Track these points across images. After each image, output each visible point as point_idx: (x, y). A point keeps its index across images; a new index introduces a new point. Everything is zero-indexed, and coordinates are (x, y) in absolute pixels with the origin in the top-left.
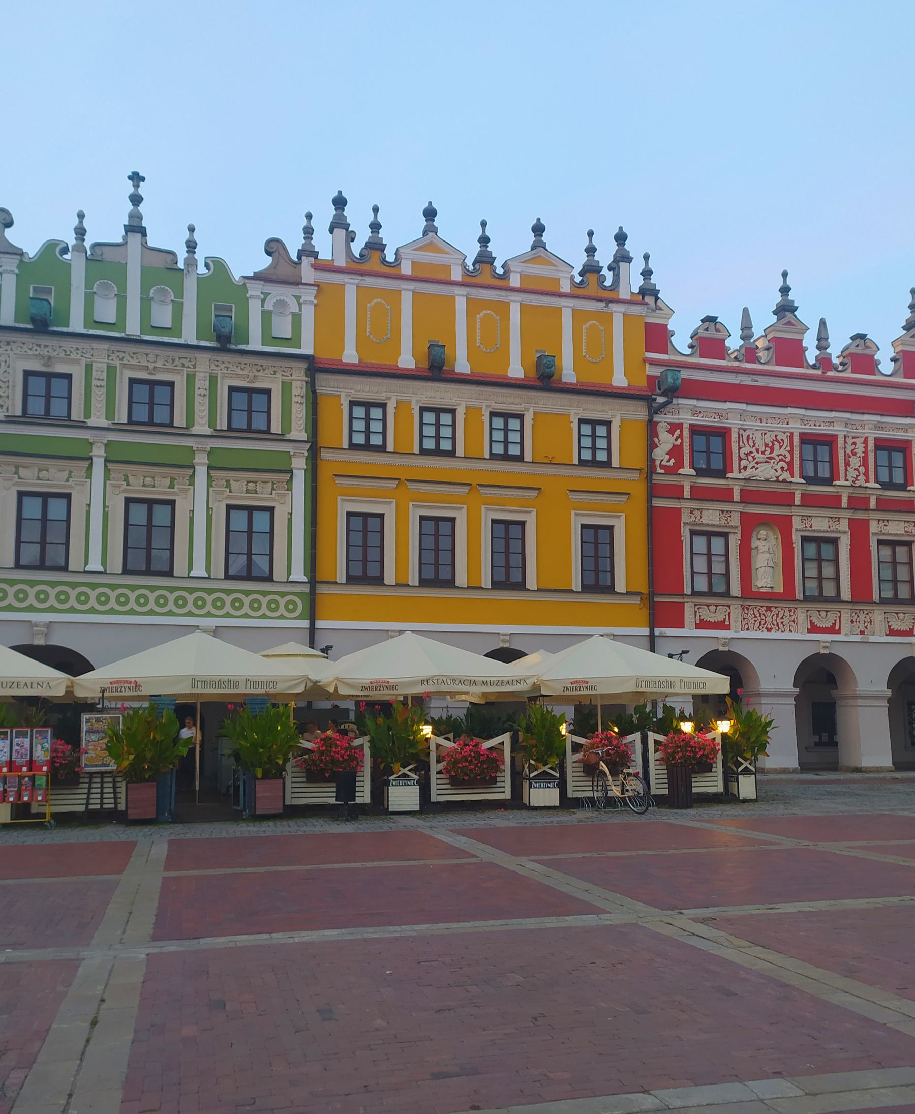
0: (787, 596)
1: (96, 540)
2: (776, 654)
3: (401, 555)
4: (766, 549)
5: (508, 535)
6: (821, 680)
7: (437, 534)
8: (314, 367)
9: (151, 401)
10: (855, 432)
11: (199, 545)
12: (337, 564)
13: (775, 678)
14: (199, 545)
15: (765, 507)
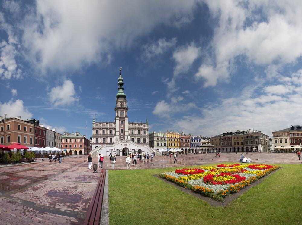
0: (184, 147)
1: (160, 145)
2: (184, 149)
3: (170, 145)
4: (184, 144)
5: (174, 144)
6: (186, 150)
7: (172, 144)
8: (167, 137)
9: (161, 139)
10: (187, 140)
11: (163, 145)
12: (168, 145)
13: (184, 149)
14: (163, 145)
15: (184, 143)
